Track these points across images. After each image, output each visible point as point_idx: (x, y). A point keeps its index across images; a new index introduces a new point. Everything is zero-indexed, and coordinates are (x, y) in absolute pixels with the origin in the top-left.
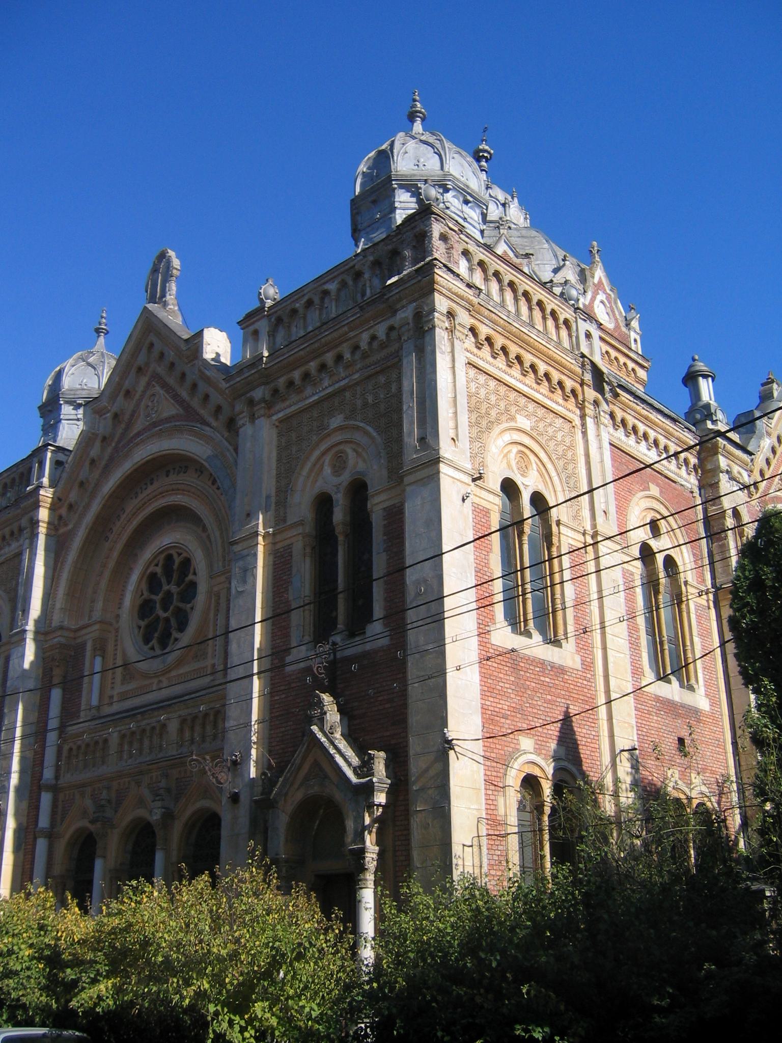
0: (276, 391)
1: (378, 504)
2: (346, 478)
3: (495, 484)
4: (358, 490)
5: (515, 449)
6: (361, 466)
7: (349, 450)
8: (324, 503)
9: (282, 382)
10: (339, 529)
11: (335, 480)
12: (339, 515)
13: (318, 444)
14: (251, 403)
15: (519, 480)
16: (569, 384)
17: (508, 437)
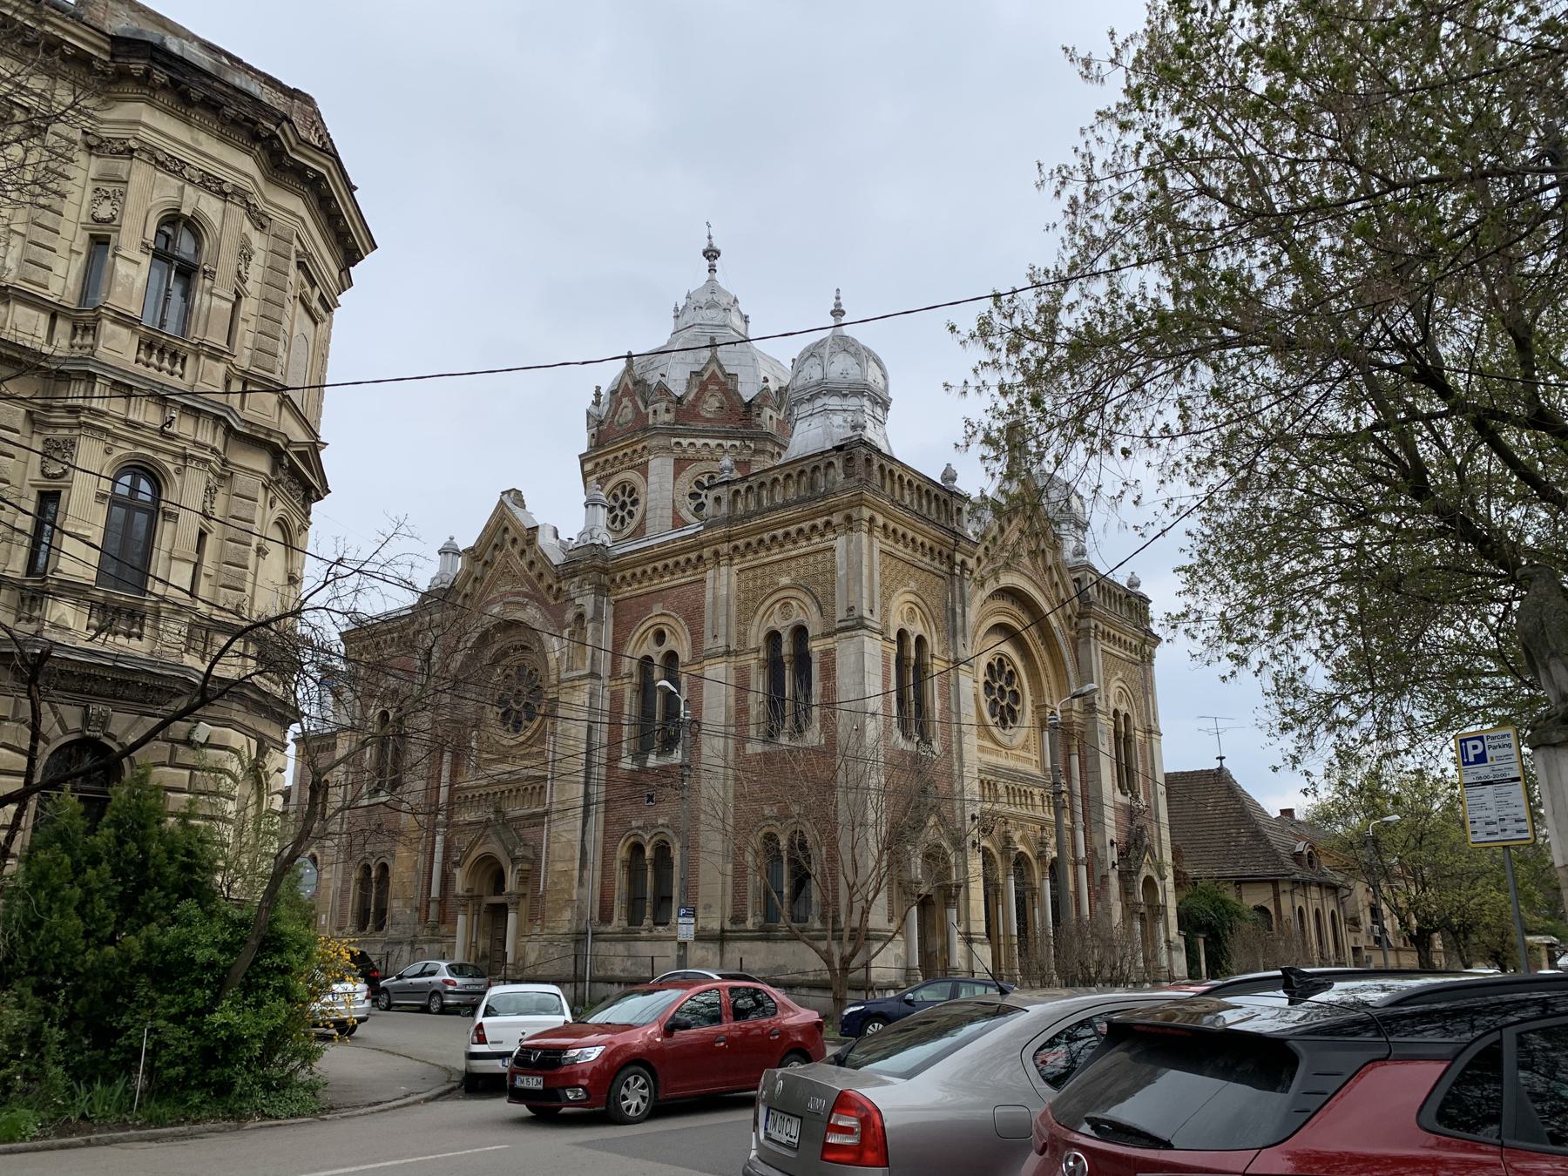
0: (736, 548)
1: (815, 647)
2: (792, 621)
3: (894, 636)
4: (800, 632)
6: (802, 617)
7: (794, 603)
8: (773, 637)
9: (741, 543)
10: (786, 659)
11: (785, 623)
12: (786, 648)
13: (770, 595)
14: (716, 553)
15: (909, 628)
16: (945, 552)
17: (902, 599)
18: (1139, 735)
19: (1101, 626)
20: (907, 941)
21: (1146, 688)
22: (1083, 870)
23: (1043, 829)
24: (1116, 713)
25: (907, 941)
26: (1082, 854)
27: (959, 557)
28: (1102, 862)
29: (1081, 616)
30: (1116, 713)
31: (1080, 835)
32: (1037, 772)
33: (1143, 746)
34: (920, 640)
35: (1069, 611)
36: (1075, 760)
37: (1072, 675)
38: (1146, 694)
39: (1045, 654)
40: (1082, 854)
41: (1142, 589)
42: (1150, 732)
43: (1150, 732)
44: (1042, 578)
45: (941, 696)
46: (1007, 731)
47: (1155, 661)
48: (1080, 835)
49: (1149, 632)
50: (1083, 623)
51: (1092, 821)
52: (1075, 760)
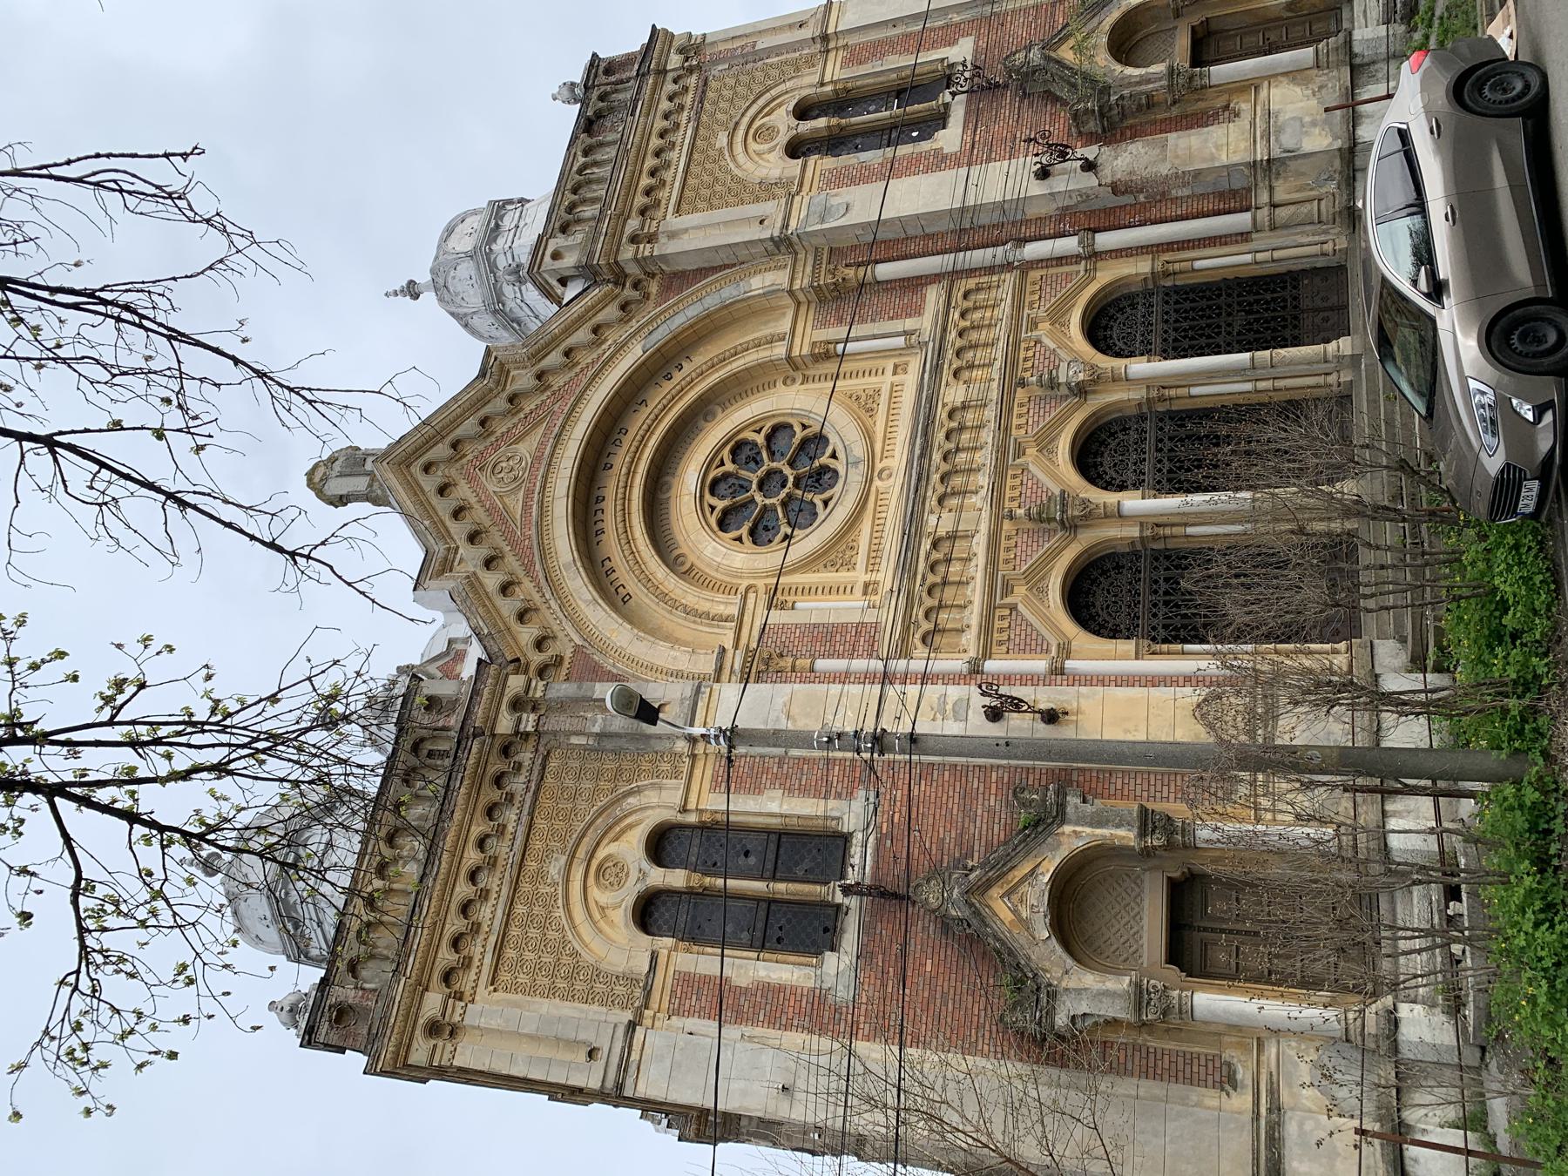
5: (595, 893)
18: (836, 71)
19: (633, 224)
20: (1272, 77)
21: (746, 54)
22: (1105, 240)
23: (1022, 383)
24: (795, 149)
25: (1272, 77)
26: (1069, 245)
27: (505, 724)
28: (1085, 196)
29: (619, 277)
30: (795, 149)
31: (1033, 250)
32: (915, 365)
33: (855, 56)
34: (660, 845)
35: (611, 312)
36: (885, 271)
37: (729, 293)
38: (758, 56)
39: (700, 359)
40: (1069, 245)
41: (578, 77)
42: (825, 38)
43: (825, 38)
44: (558, 396)
45: (757, 789)
46: (840, 467)
47: (697, 32)
48: (1033, 250)
49: (648, 48)
50: (633, 270)
51: (1009, 226)
52: (885, 271)
